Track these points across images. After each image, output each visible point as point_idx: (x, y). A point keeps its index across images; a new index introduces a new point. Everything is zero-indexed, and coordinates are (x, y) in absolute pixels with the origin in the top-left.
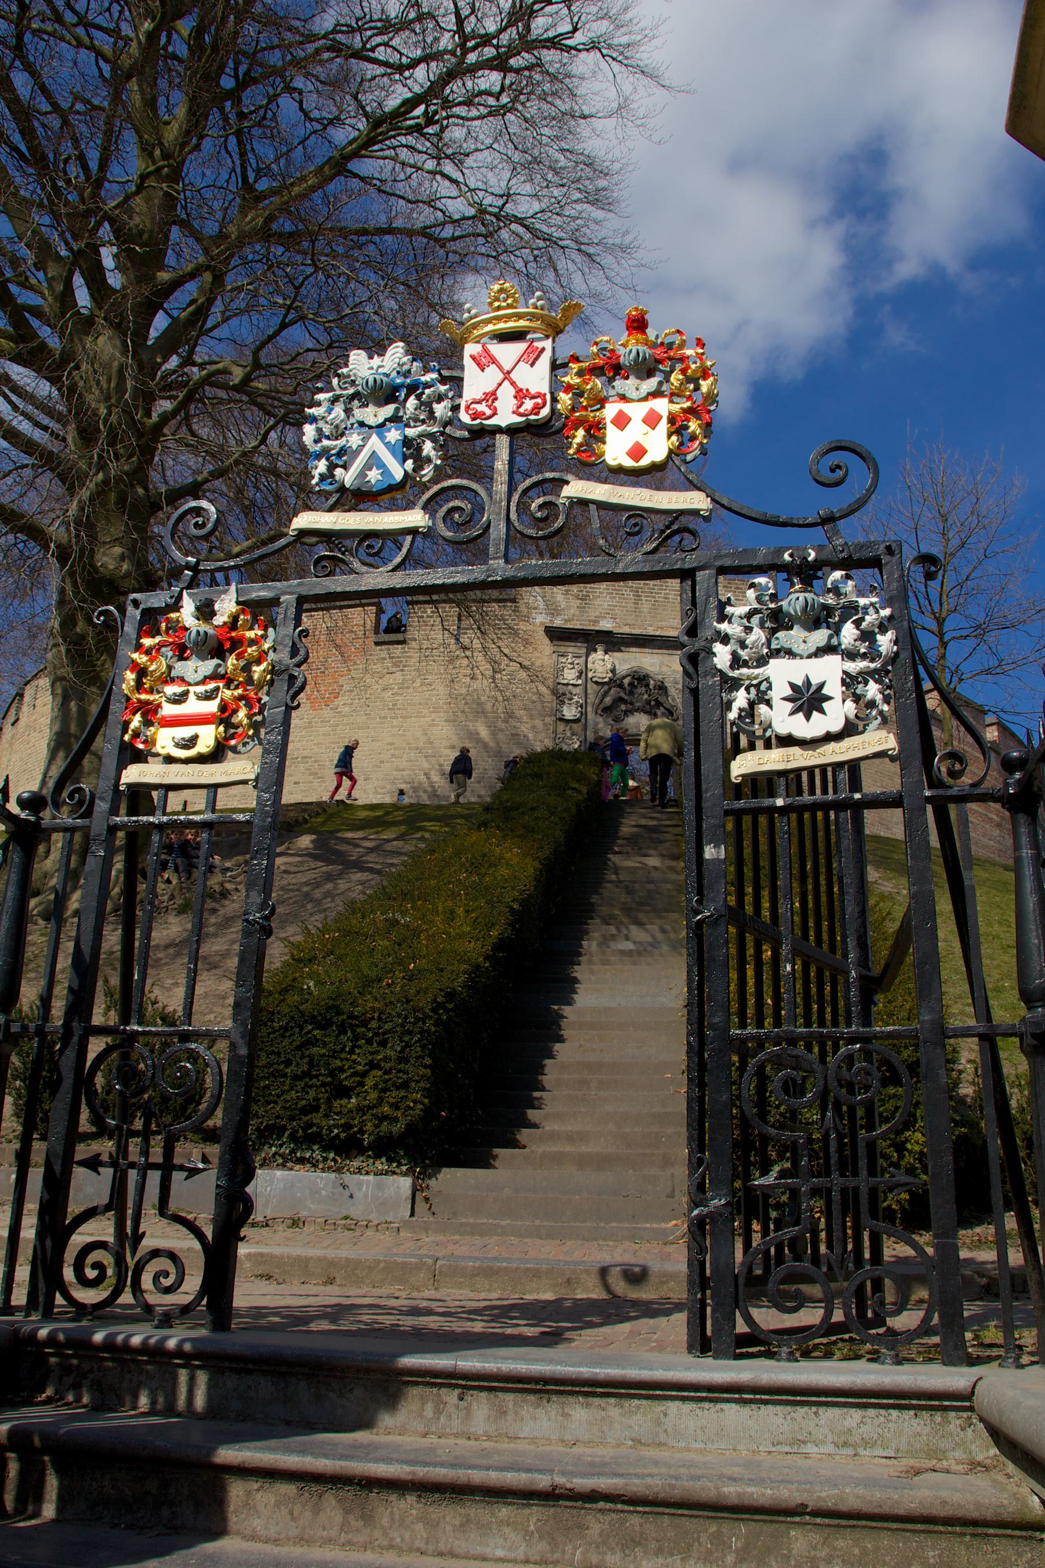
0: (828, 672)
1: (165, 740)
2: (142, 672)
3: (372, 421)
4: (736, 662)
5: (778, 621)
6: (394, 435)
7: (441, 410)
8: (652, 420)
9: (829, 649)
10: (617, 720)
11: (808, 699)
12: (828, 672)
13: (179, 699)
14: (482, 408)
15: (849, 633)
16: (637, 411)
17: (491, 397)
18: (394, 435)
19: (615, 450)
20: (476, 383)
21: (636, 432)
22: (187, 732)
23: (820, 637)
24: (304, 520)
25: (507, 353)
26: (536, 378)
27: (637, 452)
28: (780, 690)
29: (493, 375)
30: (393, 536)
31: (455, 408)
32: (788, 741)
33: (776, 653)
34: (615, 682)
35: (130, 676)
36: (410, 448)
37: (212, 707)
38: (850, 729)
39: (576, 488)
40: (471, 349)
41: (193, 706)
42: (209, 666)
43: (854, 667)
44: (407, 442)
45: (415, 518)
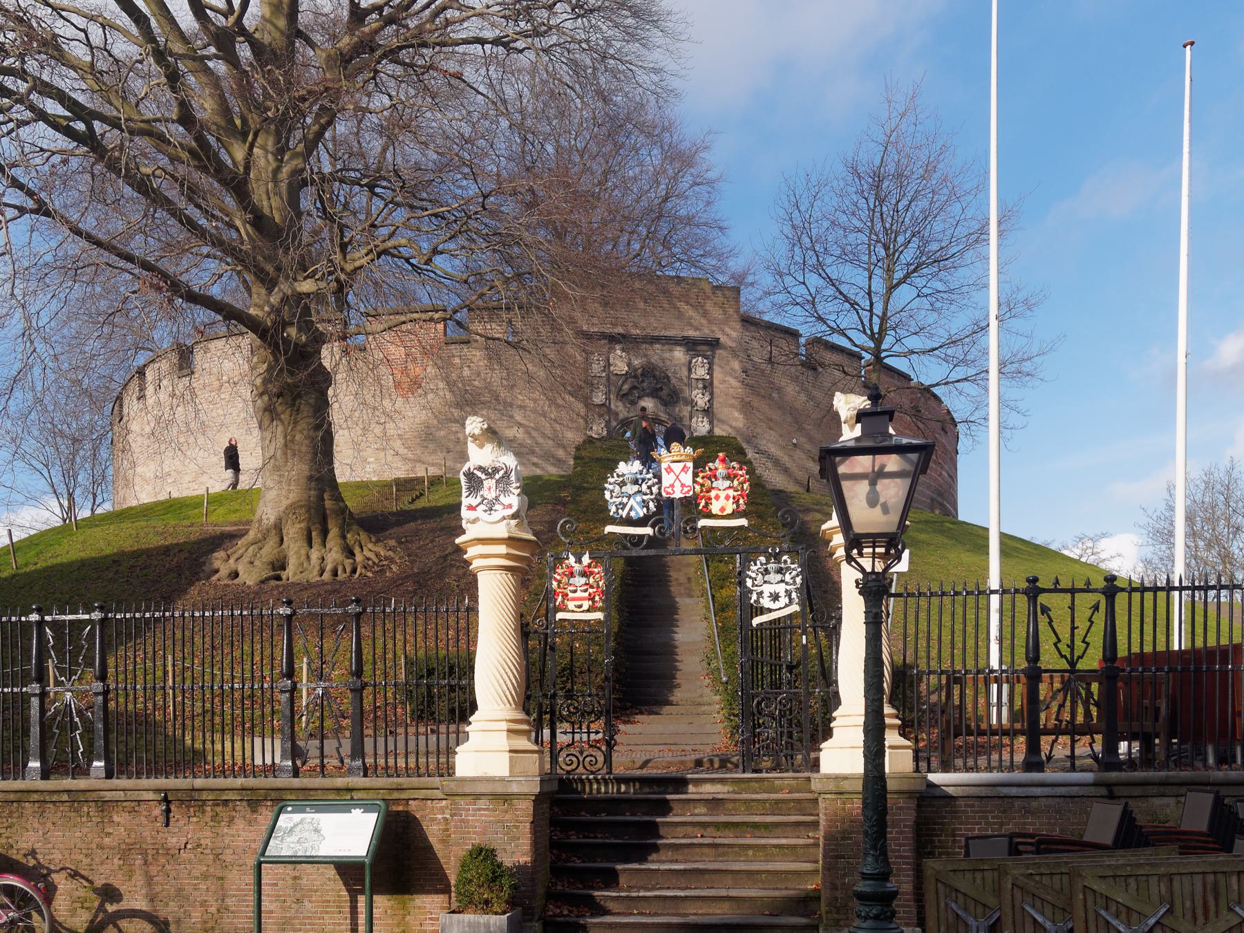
0: (781, 589)
1: (571, 605)
2: (559, 582)
5: (767, 572)
6: (639, 498)
7: (655, 489)
8: (727, 498)
9: (782, 581)
10: (633, 403)
11: (775, 597)
12: (781, 589)
13: (575, 591)
14: (670, 490)
15: (788, 577)
17: (672, 486)
19: (715, 508)
20: (667, 479)
21: (722, 502)
23: (779, 577)
24: (609, 529)
25: (677, 467)
26: (687, 478)
27: (723, 509)
28: (766, 594)
29: (672, 476)
30: (641, 537)
31: (660, 489)
33: (765, 582)
34: (632, 374)
35: (555, 584)
36: (645, 504)
37: (586, 594)
38: (787, 606)
39: (703, 523)
40: (664, 466)
41: (579, 594)
42: (583, 580)
43: (788, 588)
44: (644, 501)
45: (648, 531)
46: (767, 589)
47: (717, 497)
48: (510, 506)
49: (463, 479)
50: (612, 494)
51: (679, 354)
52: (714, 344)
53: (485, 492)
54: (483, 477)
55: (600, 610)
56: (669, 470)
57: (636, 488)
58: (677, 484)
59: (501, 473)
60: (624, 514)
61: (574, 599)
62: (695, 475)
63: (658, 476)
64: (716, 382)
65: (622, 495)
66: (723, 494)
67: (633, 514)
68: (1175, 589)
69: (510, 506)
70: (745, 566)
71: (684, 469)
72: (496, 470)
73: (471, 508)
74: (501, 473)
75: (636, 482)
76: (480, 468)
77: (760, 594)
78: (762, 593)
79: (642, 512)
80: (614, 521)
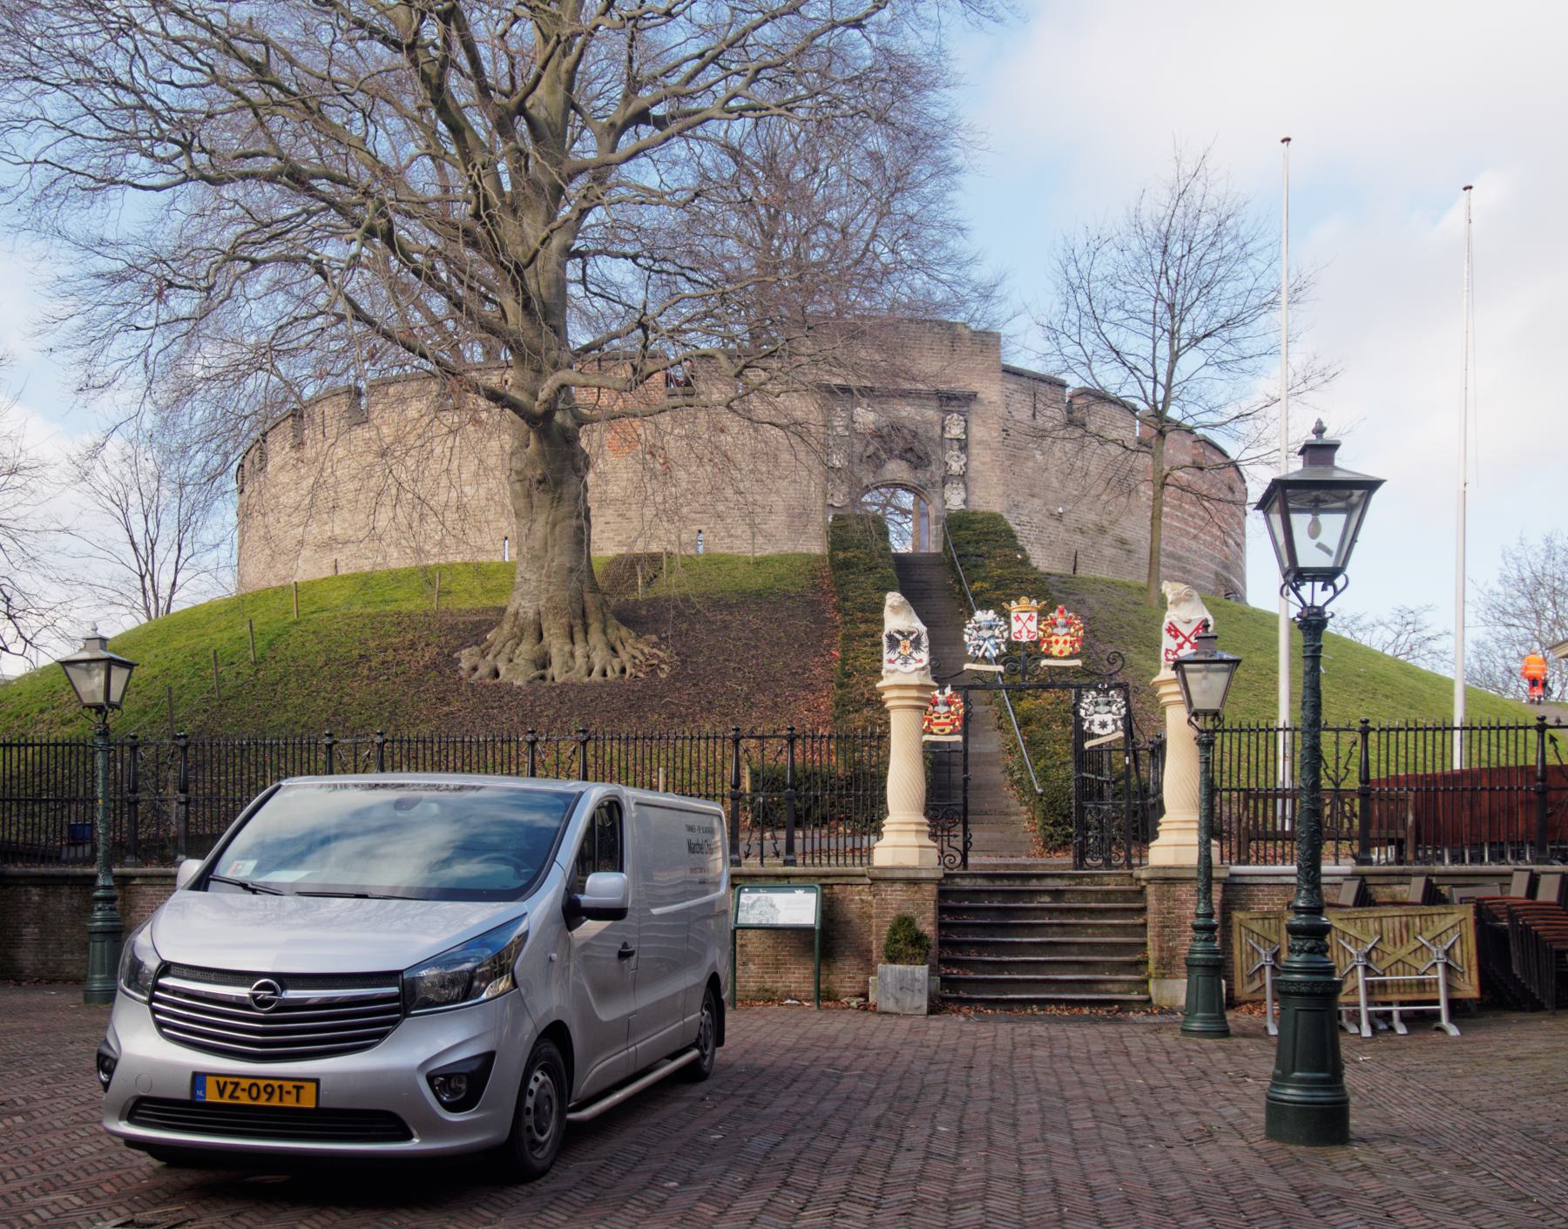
0: (1109, 718)
5: (1097, 704)
11: (1103, 725)
12: (1109, 718)
15: (1114, 708)
20: (1016, 626)
21: (1060, 646)
24: (967, 666)
25: (1024, 617)
26: (1033, 626)
36: (997, 646)
39: (1044, 662)
40: (1013, 615)
46: (1097, 718)
49: (885, 640)
50: (969, 637)
51: (931, 414)
52: (972, 397)
53: (900, 649)
56: (1018, 619)
57: (990, 633)
58: (1025, 632)
62: (1039, 622)
63: (1008, 623)
64: (972, 442)
65: (979, 638)
70: (1079, 698)
71: (1030, 618)
72: (911, 633)
73: (891, 661)
75: (990, 628)
76: (899, 632)
77: (1091, 723)
79: (995, 653)
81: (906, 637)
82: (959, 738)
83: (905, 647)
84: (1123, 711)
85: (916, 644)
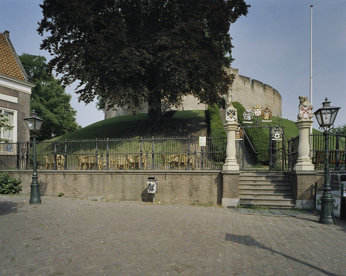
3: (248, 115)
4: (273, 133)
6: (250, 116)
7: (253, 114)
8: (268, 116)
11: (277, 136)
16: (267, 115)
17: (257, 114)
18: (250, 116)
22: (237, 137)
24: (244, 122)
25: (258, 110)
26: (260, 112)
32: (276, 138)
33: (275, 133)
36: (251, 117)
41: (238, 135)
45: (252, 122)
47: (266, 116)
48: (235, 118)
54: (230, 112)
55: (242, 138)
58: (258, 113)
59: (234, 112)
60: (247, 119)
61: (237, 136)
66: (267, 115)
67: (249, 119)
68: (312, 135)
69: (235, 118)
71: (259, 110)
72: (233, 111)
73: (227, 118)
74: (234, 112)
77: (274, 135)
78: (275, 135)
79: (250, 119)
80: (245, 121)
81: (231, 112)
82: (242, 139)
83: (231, 115)
84: (282, 133)
85: (234, 114)
